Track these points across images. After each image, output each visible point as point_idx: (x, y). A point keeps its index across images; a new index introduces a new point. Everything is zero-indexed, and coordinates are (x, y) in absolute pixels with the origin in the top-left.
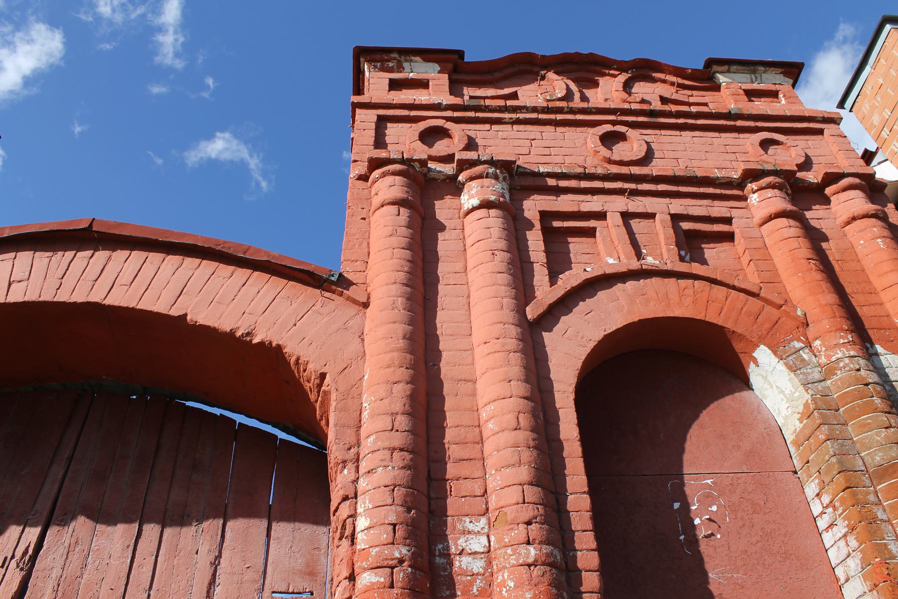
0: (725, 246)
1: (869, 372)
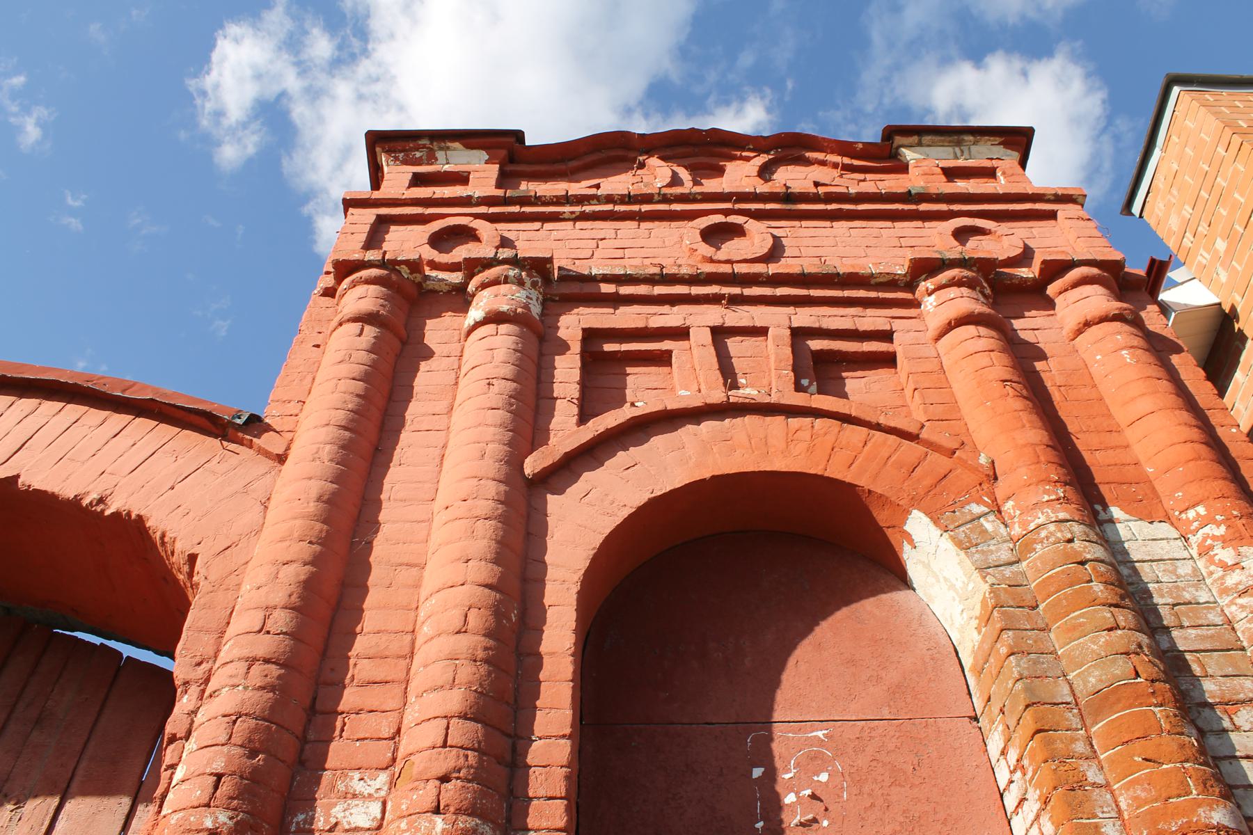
0: (883, 374)
1: (1087, 544)
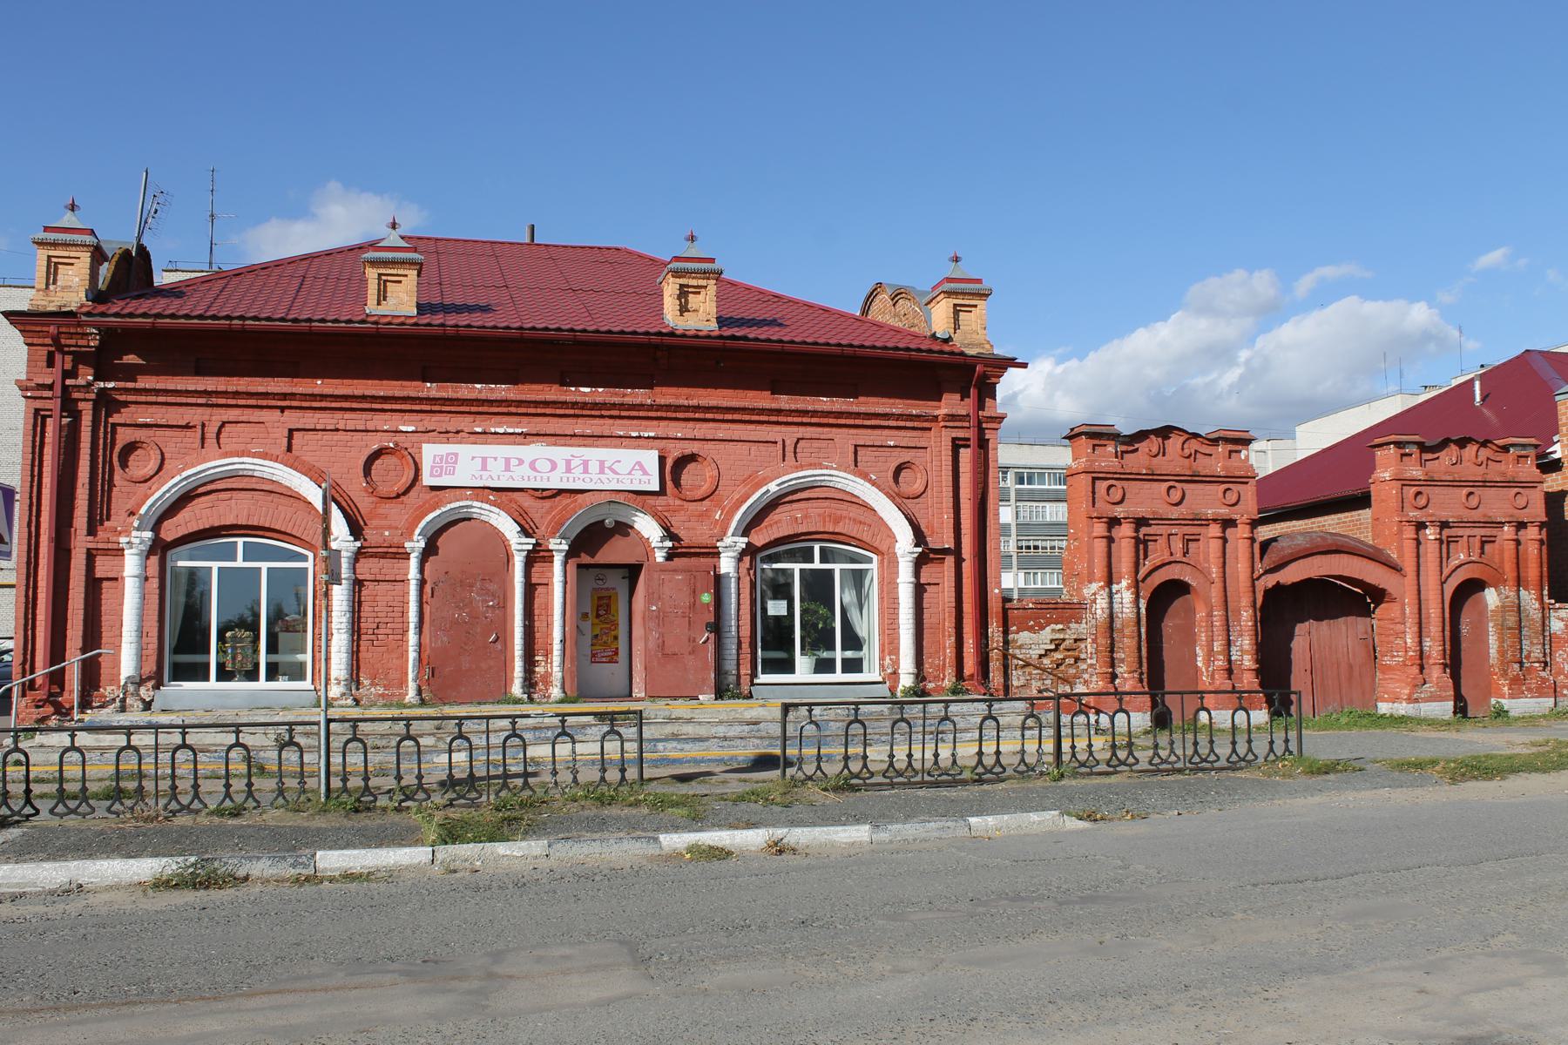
0: (1491, 545)
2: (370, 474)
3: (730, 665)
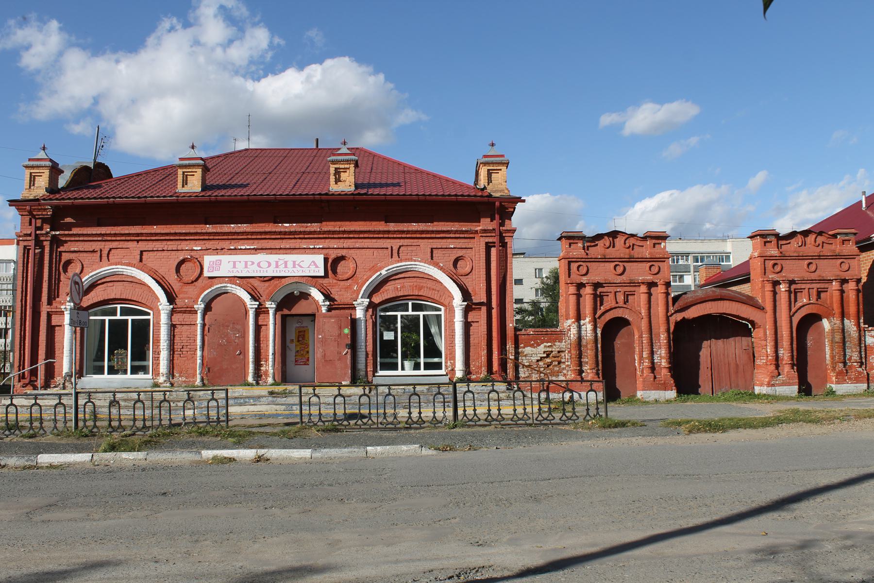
0: (825, 293)
2: (179, 272)
3: (361, 365)
